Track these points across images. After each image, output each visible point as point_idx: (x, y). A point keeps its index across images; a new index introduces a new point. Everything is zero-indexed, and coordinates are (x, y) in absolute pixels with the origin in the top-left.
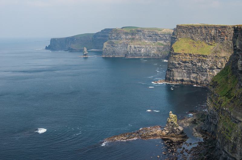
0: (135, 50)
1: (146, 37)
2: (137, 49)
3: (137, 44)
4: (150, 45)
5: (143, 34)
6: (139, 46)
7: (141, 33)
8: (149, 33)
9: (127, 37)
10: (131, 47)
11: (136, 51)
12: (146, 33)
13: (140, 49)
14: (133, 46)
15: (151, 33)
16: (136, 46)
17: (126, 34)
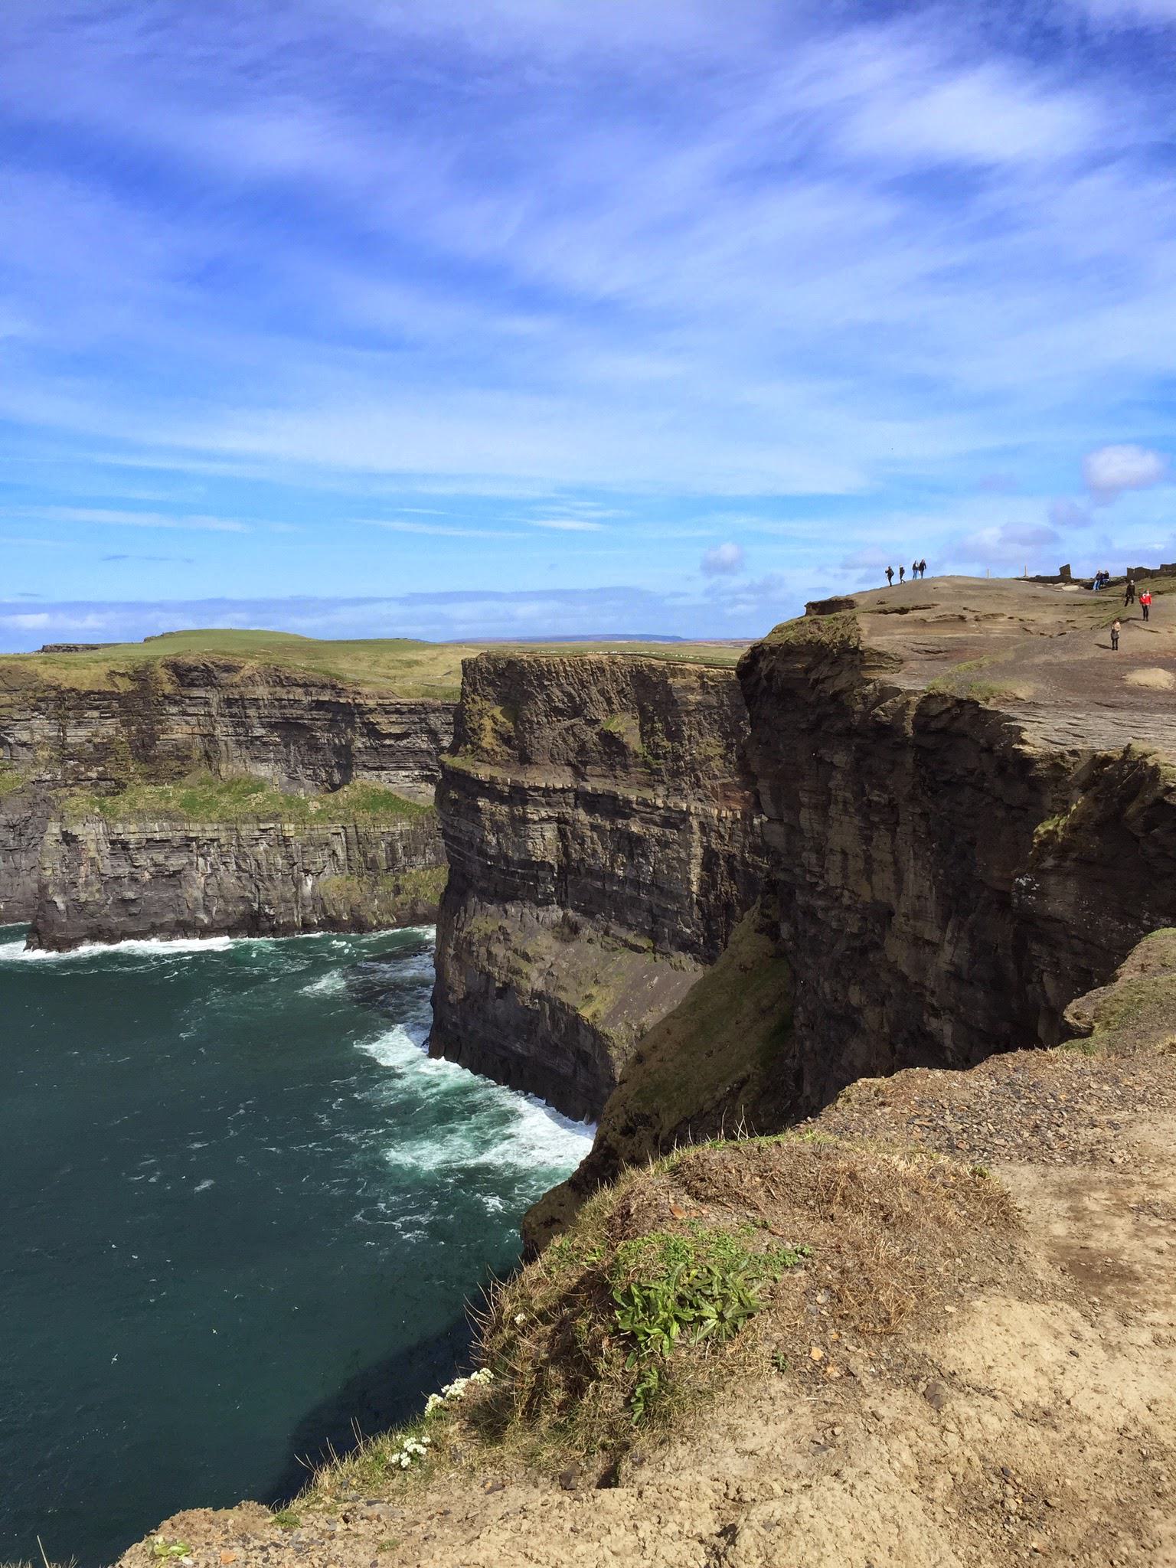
0: (124, 870)
1: (259, 732)
2: (142, 859)
3: (140, 815)
4: (275, 817)
5: (229, 703)
6: (157, 829)
7: (214, 697)
8: (281, 692)
9: (76, 736)
10: (68, 839)
11: (134, 880)
12: (262, 692)
13: (176, 862)
14: (91, 833)
15: (298, 693)
16: (131, 832)
17: (66, 703)
